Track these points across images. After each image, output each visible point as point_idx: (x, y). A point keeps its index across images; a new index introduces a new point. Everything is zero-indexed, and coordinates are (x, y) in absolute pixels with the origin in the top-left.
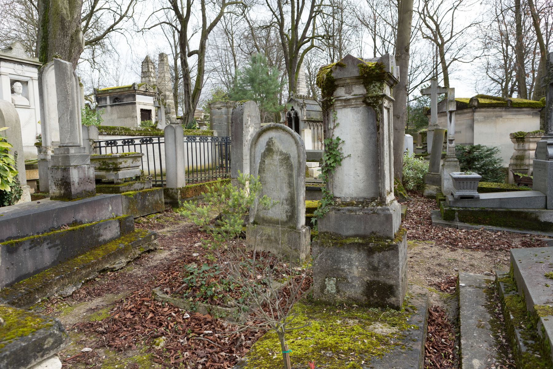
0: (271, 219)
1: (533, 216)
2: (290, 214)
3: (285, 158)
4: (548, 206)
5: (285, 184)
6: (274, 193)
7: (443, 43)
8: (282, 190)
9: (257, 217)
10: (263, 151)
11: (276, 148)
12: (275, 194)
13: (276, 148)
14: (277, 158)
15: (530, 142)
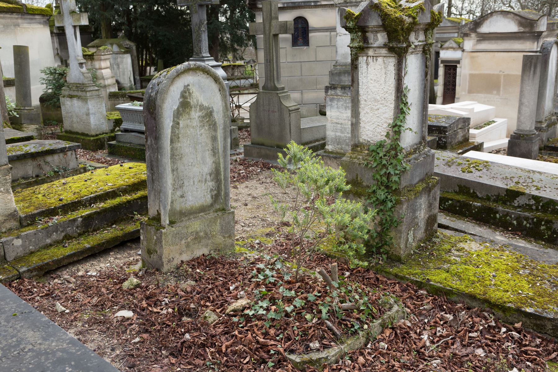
2: (215, 192)
5: (207, 152)
6: (195, 169)
8: (204, 162)
9: (173, 213)
10: (175, 108)
11: (195, 100)
12: (196, 170)
13: (195, 100)
14: (195, 114)
15: (101, 60)
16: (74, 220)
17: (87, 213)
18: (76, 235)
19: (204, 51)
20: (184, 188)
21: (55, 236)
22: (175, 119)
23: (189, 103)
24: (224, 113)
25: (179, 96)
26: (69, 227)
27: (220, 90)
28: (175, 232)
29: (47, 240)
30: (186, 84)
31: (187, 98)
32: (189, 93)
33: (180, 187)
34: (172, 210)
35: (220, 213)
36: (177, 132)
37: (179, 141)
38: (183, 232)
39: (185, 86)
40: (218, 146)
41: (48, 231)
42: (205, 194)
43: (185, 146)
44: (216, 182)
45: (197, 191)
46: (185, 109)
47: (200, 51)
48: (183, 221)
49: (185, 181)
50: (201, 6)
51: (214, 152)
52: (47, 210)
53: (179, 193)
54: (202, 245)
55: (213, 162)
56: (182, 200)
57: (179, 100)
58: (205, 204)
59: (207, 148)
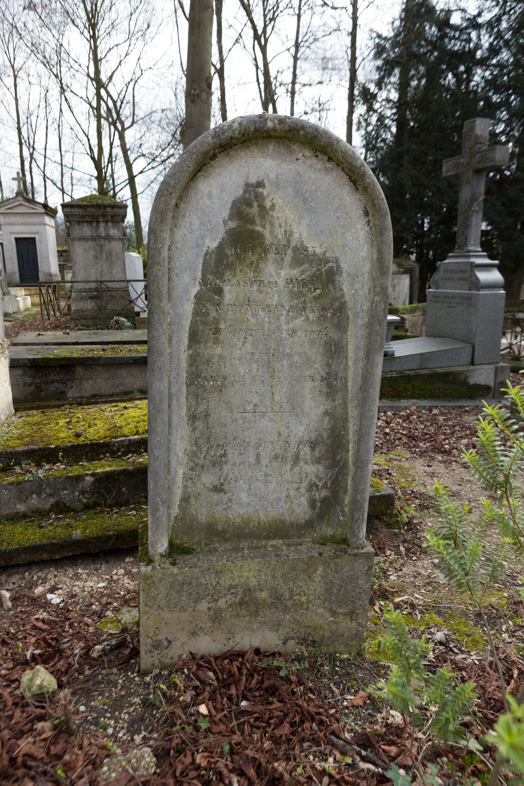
0: (246, 522)
1: (462, 377)
2: (324, 493)
3: (315, 278)
4: (475, 360)
5: (309, 385)
6: (264, 423)
7: (124, 129)
9: (184, 524)
10: (214, 245)
11: (280, 233)
12: (267, 426)
14: (278, 274)
16: (78, 478)
17: (108, 469)
18: (78, 505)
19: (472, 243)
20: (226, 468)
21: (34, 501)
22: (210, 277)
23: (260, 236)
24: (374, 280)
25: (226, 213)
26: (64, 489)
27: (366, 214)
28: (180, 578)
29: (19, 506)
30: (253, 180)
31: (253, 223)
32: (262, 207)
33: (214, 464)
34: (183, 519)
35: (328, 550)
36: (213, 314)
37: (216, 341)
38: (203, 581)
39: (247, 185)
40: (346, 370)
41: (21, 490)
42: (292, 493)
43: (236, 356)
44: (331, 467)
45: (266, 482)
46: (245, 251)
47: (466, 242)
48: (216, 550)
49: (230, 451)
50: (478, 172)
51: (332, 385)
52: (40, 449)
53: (208, 479)
54: (262, 623)
55: (326, 413)
56: (216, 497)
57: (225, 222)
58: (288, 519)
59: (308, 373)
